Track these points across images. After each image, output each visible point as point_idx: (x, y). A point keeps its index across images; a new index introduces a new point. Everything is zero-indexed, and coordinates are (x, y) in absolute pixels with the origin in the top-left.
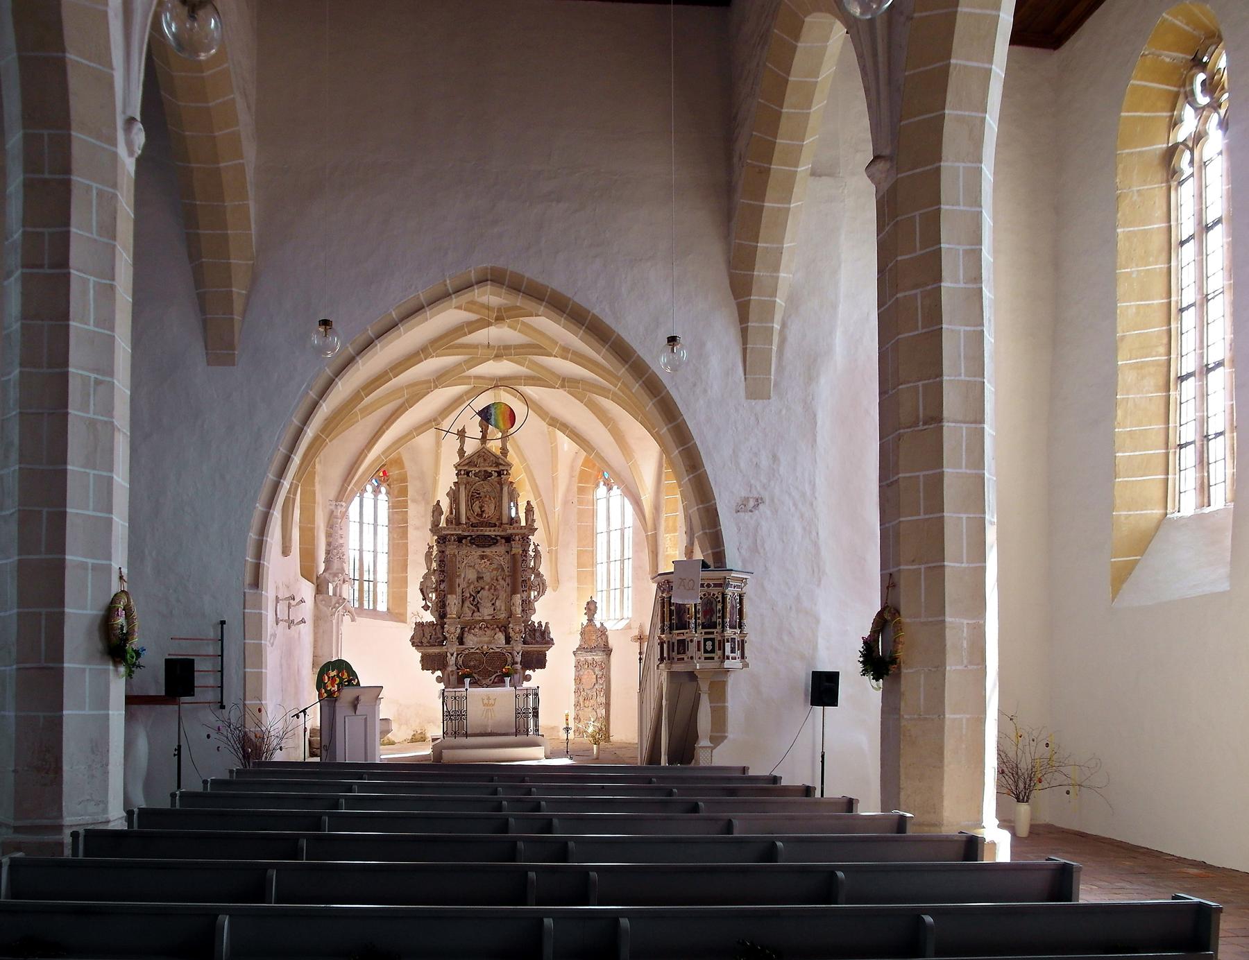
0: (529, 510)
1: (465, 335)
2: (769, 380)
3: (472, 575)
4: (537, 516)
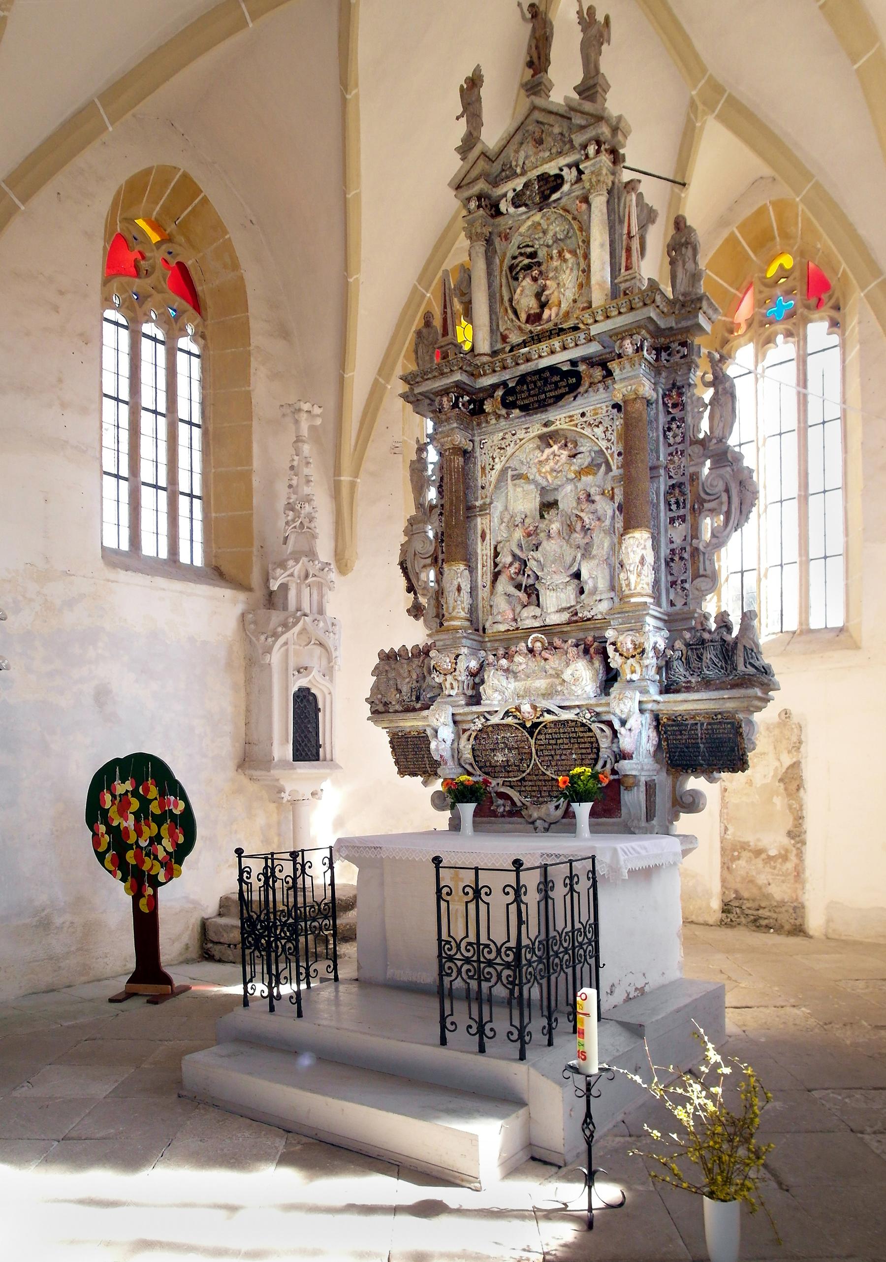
3: (523, 501)
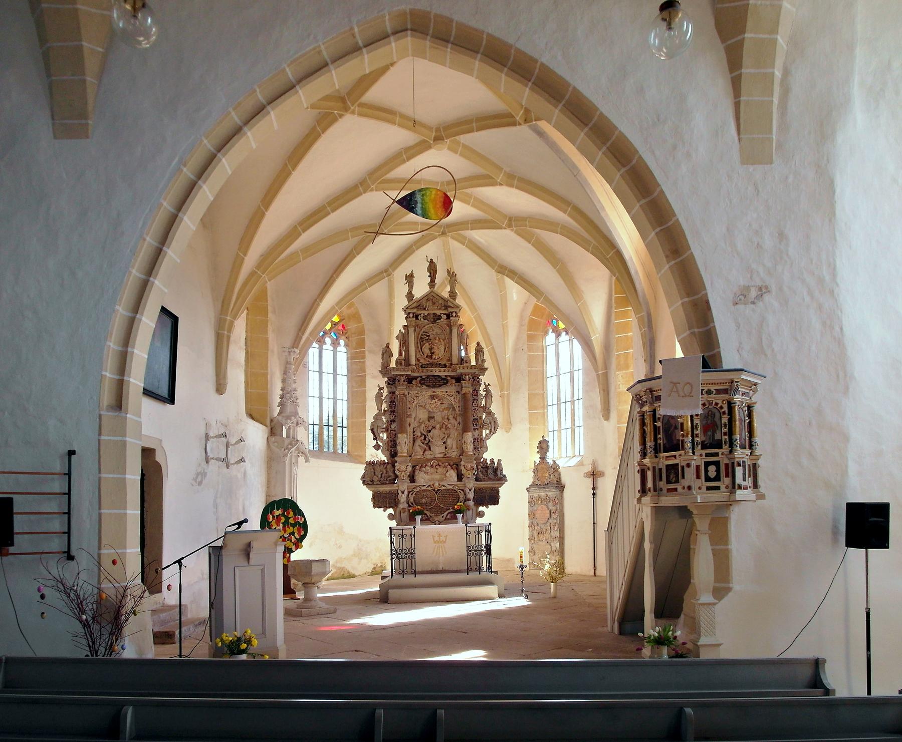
0: (479, 351)
1: (404, 162)
2: (770, 140)
3: (423, 415)
4: (487, 356)
